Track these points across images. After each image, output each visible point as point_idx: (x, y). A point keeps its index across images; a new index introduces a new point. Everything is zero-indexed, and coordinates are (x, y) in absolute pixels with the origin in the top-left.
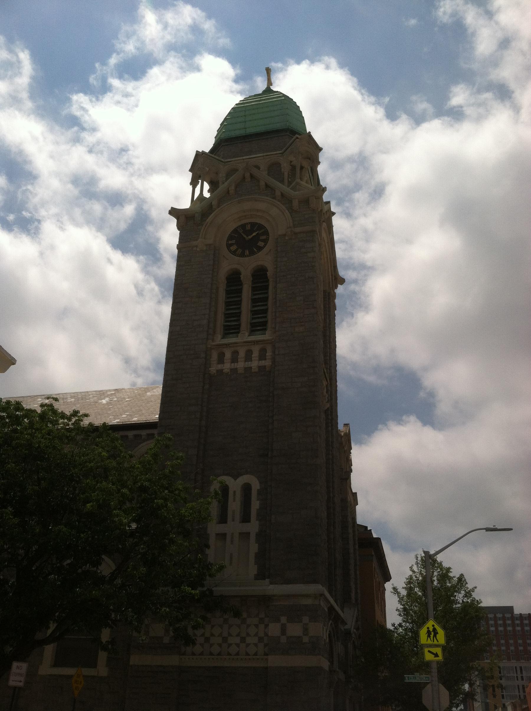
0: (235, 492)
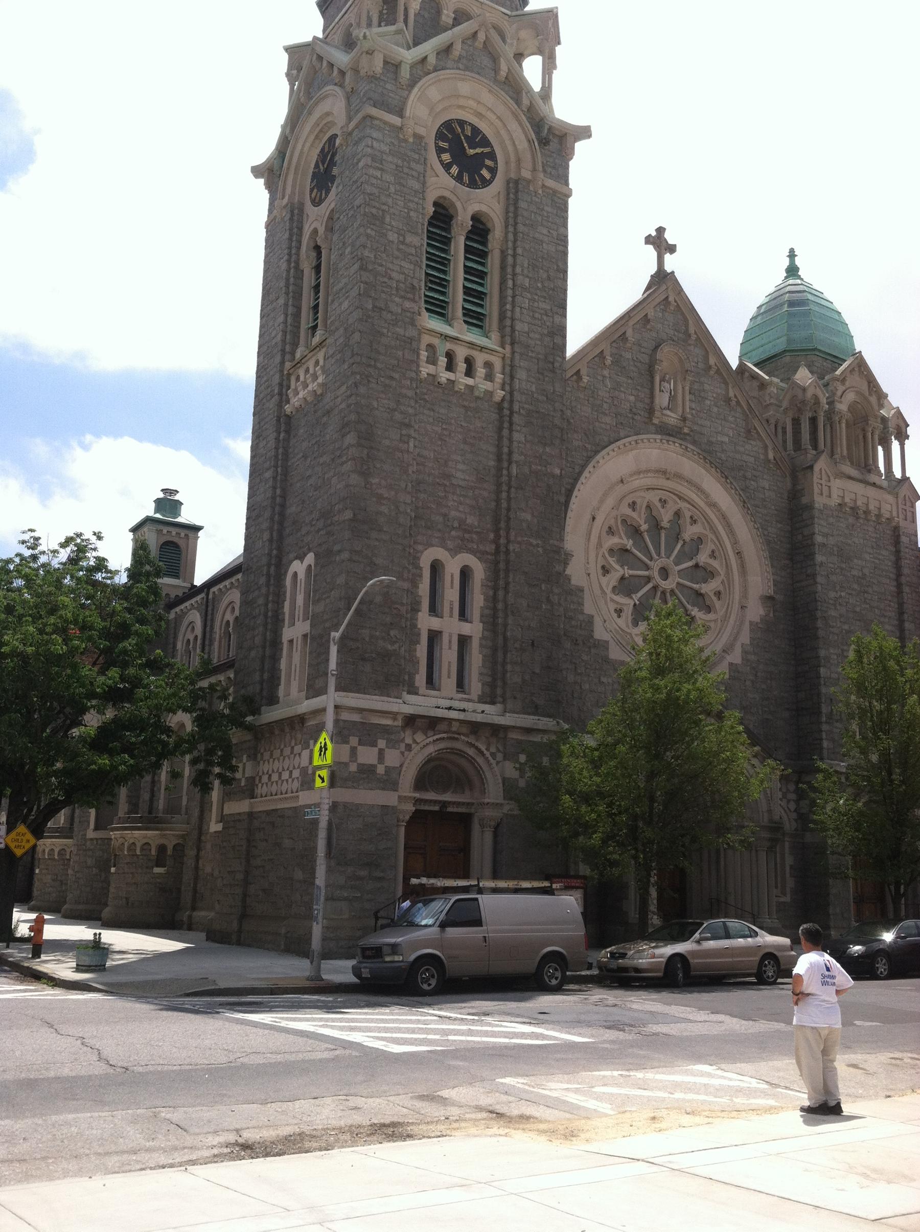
0: (452, 576)
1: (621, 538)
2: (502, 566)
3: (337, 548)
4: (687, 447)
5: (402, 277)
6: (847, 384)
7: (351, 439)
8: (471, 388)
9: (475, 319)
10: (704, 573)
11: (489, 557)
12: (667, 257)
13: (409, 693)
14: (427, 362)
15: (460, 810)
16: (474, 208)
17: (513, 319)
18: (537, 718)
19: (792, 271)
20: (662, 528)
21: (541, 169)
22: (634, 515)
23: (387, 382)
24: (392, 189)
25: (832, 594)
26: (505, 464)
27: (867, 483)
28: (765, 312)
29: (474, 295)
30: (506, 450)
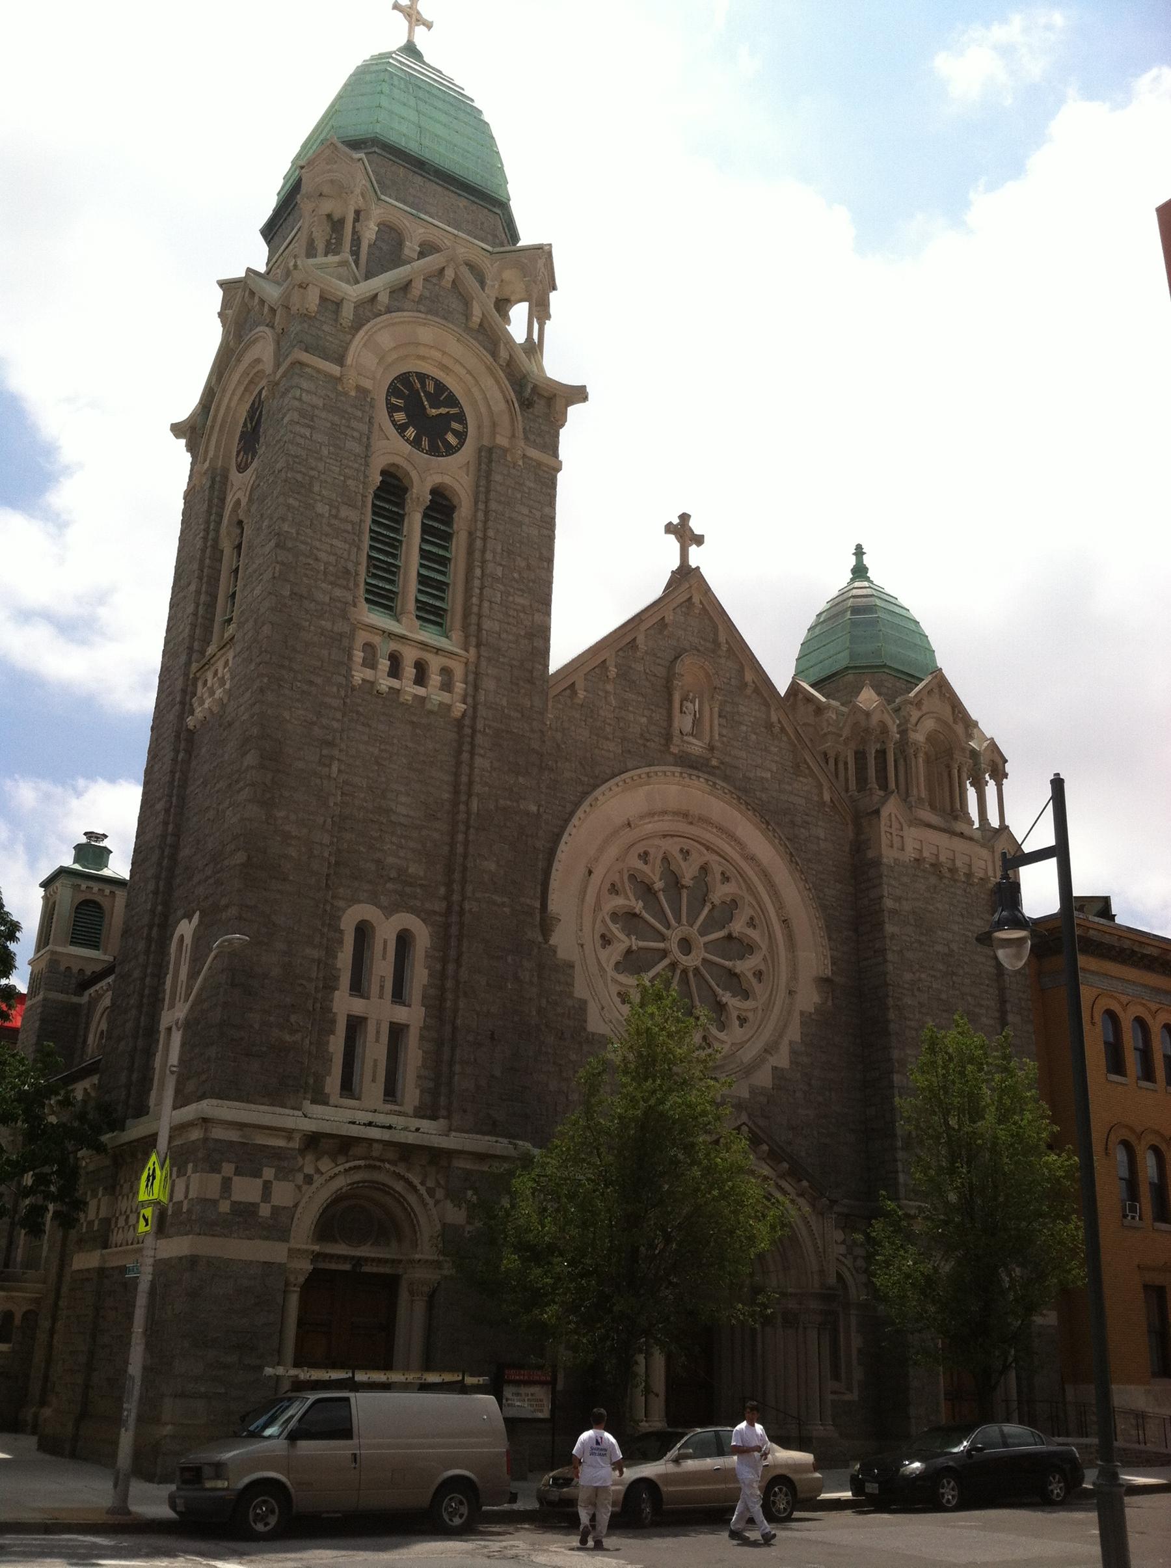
0: (385, 942)
1: (627, 898)
2: (454, 930)
3: (223, 902)
4: (715, 784)
5: (332, 559)
6: (925, 709)
7: (251, 759)
8: (422, 700)
9: (432, 614)
10: (741, 947)
11: (438, 918)
12: (693, 550)
13: (313, 1102)
14: (364, 664)
16: (437, 479)
17: (480, 616)
18: (494, 1139)
19: (860, 571)
20: (683, 886)
21: (521, 435)
22: (646, 868)
23: (305, 687)
24: (325, 452)
25: (908, 976)
26: (463, 798)
27: (953, 833)
28: (824, 621)
29: (431, 585)
30: (464, 779)
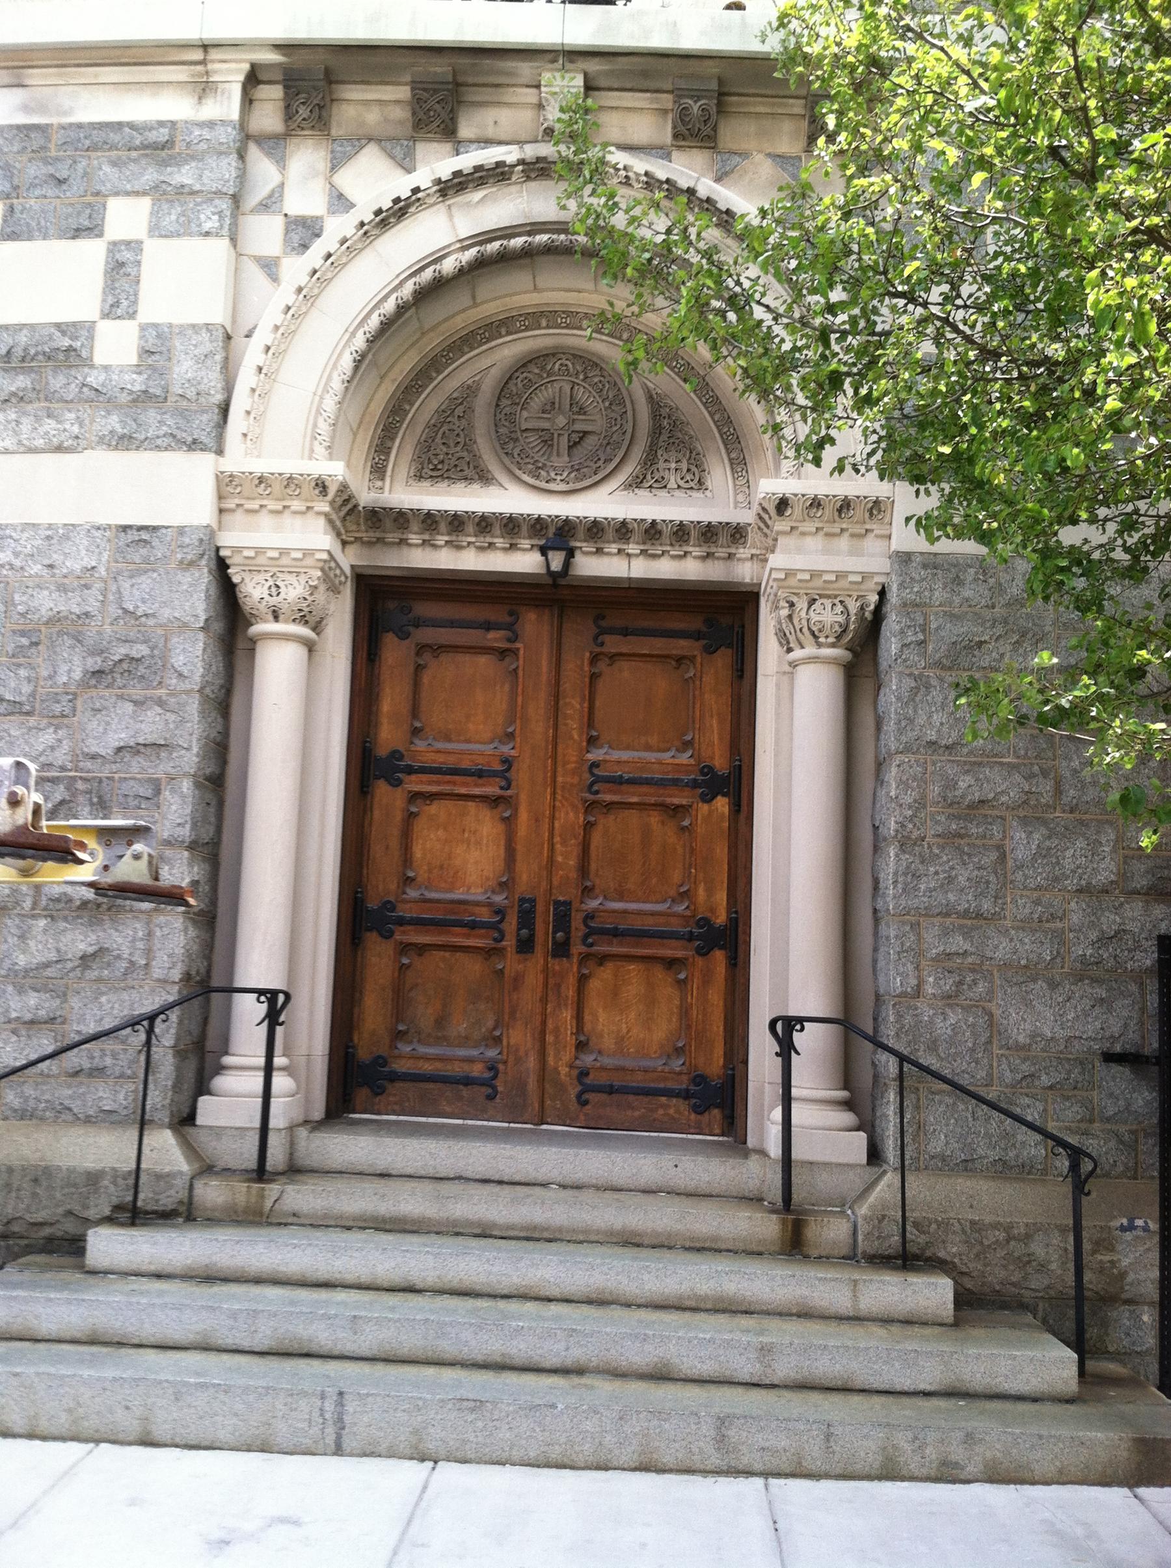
15: (666, 568)
